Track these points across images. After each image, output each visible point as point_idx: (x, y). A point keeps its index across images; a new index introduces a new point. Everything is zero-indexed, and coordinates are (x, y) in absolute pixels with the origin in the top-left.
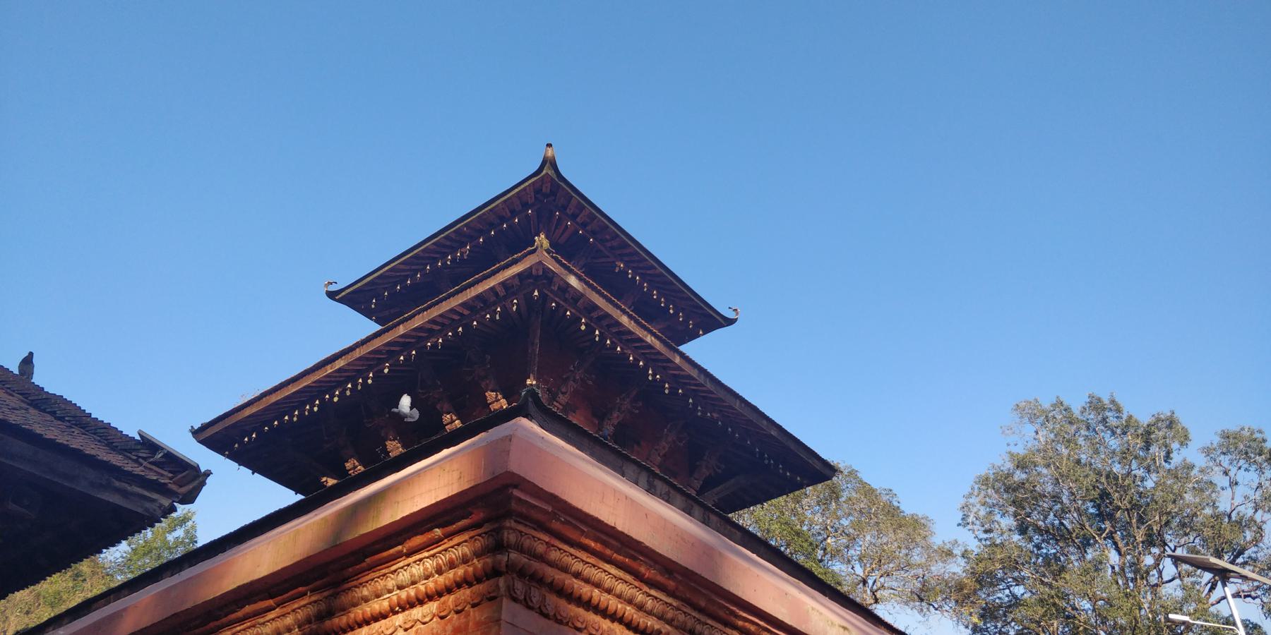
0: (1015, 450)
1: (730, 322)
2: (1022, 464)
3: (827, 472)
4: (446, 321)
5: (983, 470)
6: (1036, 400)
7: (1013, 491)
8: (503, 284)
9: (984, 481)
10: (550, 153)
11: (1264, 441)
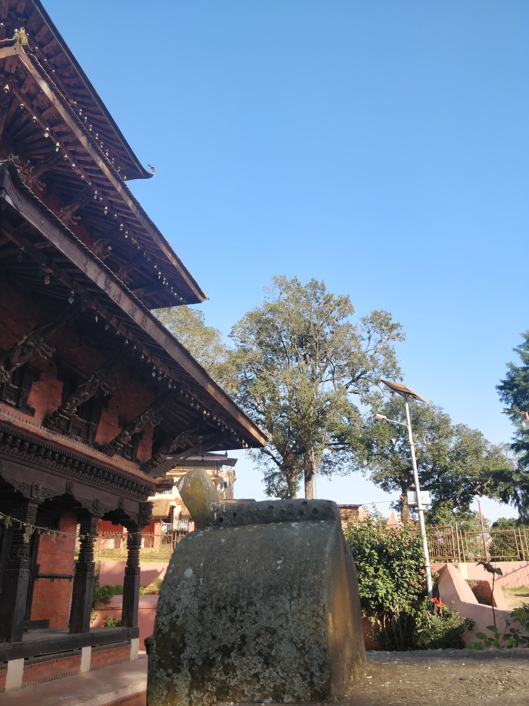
0: (269, 301)
1: (148, 176)
2: (273, 310)
3: (200, 297)
5: (251, 310)
6: (285, 276)
7: (261, 324)
9: (250, 315)
11: (391, 319)
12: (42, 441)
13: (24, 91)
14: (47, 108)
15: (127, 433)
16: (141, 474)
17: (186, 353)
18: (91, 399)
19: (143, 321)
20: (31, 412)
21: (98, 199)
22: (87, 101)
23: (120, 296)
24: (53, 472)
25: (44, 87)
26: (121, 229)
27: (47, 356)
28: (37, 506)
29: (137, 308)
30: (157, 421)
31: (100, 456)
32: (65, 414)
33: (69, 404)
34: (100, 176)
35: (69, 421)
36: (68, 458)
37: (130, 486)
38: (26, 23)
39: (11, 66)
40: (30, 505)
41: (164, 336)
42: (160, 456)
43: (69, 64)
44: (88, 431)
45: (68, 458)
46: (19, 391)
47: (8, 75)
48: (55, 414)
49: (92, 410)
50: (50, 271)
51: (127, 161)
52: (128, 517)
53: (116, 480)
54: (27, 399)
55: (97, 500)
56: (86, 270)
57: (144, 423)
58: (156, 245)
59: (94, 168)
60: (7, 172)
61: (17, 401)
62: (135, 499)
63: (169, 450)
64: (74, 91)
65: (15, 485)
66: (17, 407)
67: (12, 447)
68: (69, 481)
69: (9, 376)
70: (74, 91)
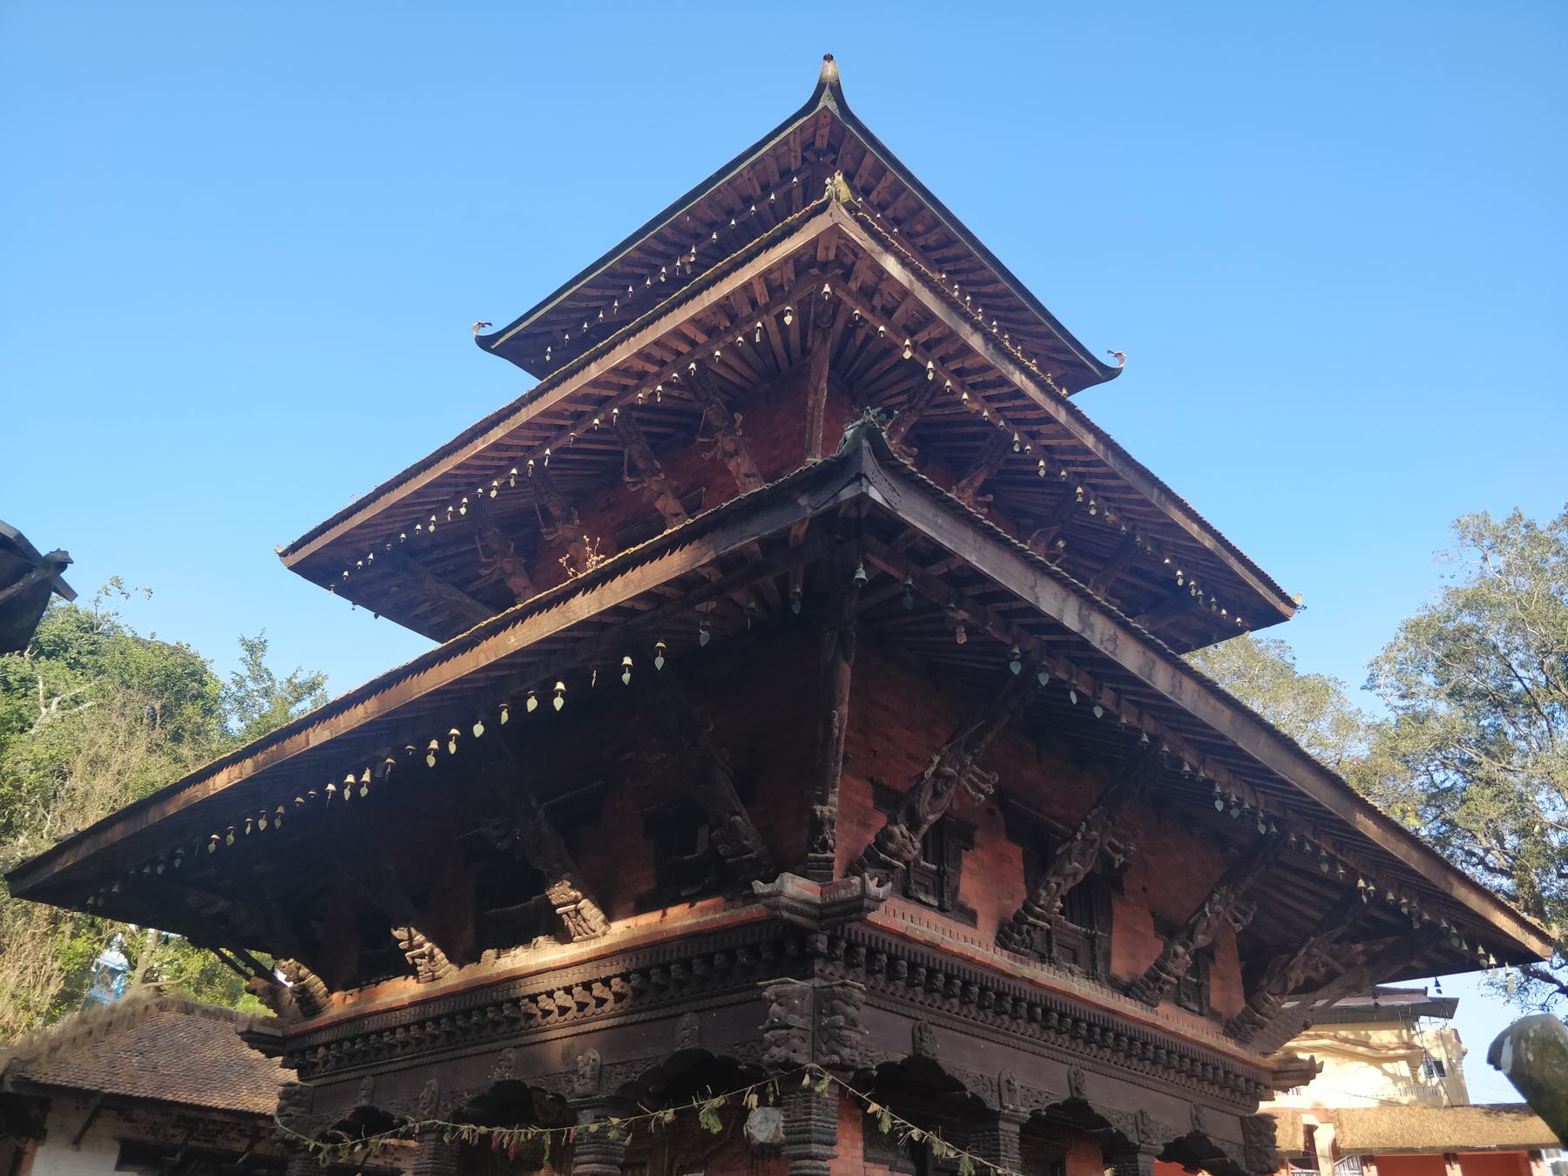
0: (1453, 584)
1: (1110, 374)
2: (1473, 603)
3: (1282, 607)
4: (669, 358)
5: (1414, 615)
6: (1485, 513)
7: (1447, 645)
8: (765, 275)
9: (1414, 628)
10: (830, 70)
12: (1002, 979)
13: (854, 286)
14: (899, 304)
15: (1180, 950)
16: (1230, 1046)
17: (1288, 745)
18: (1087, 876)
19: (1173, 685)
20: (970, 917)
21: (1022, 451)
22: (965, 265)
23: (1114, 639)
24: (1038, 1049)
25: (891, 265)
26: (1080, 499)
27: (982, 791)
28: (1017, 1129)
29: (1155, 658)
30: (1244, 914)
31: (1129, 1007)
32: (1038, 917)
33: (1043, 893)
34: (1019, 402)
35: (1048, 932)
36: (1062, 1015)
37: (1210, 1076)
38: (834, 162)
39: (827, 249)
40: (1002, 1125)
41: (1228, 713)
42: (1266, 1000)
43: (922, 207)
44: (1092, 949)
45: (1062, 1015)
46: (940, 875)
47: (824, 266)
48: (1019, 919)
49: (1093, 901)
50: (963, 615)
51: (1062, 357)
52: (1220, 1153)
53: (1176, 1063)
54: (957, 889)
55: (1142, 1113)
56: (1037, 598)
57: (1215, 923)
58: (1161, 514)
59: (1005, 390)
60: (865, 443)
61: (940, 896)
62: (1228, 1108)
63: (1285, 986)
64: (937, 254)
65: (965, 1081)
66: (941, 909)
67: (946, 997)
68: (1073, 1068)
69: (918, 845)
70: (937, 254)
